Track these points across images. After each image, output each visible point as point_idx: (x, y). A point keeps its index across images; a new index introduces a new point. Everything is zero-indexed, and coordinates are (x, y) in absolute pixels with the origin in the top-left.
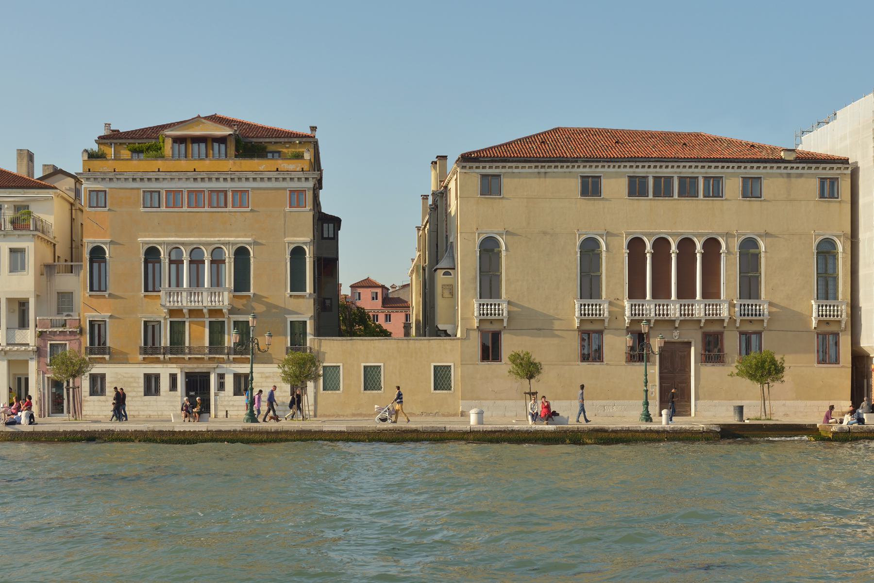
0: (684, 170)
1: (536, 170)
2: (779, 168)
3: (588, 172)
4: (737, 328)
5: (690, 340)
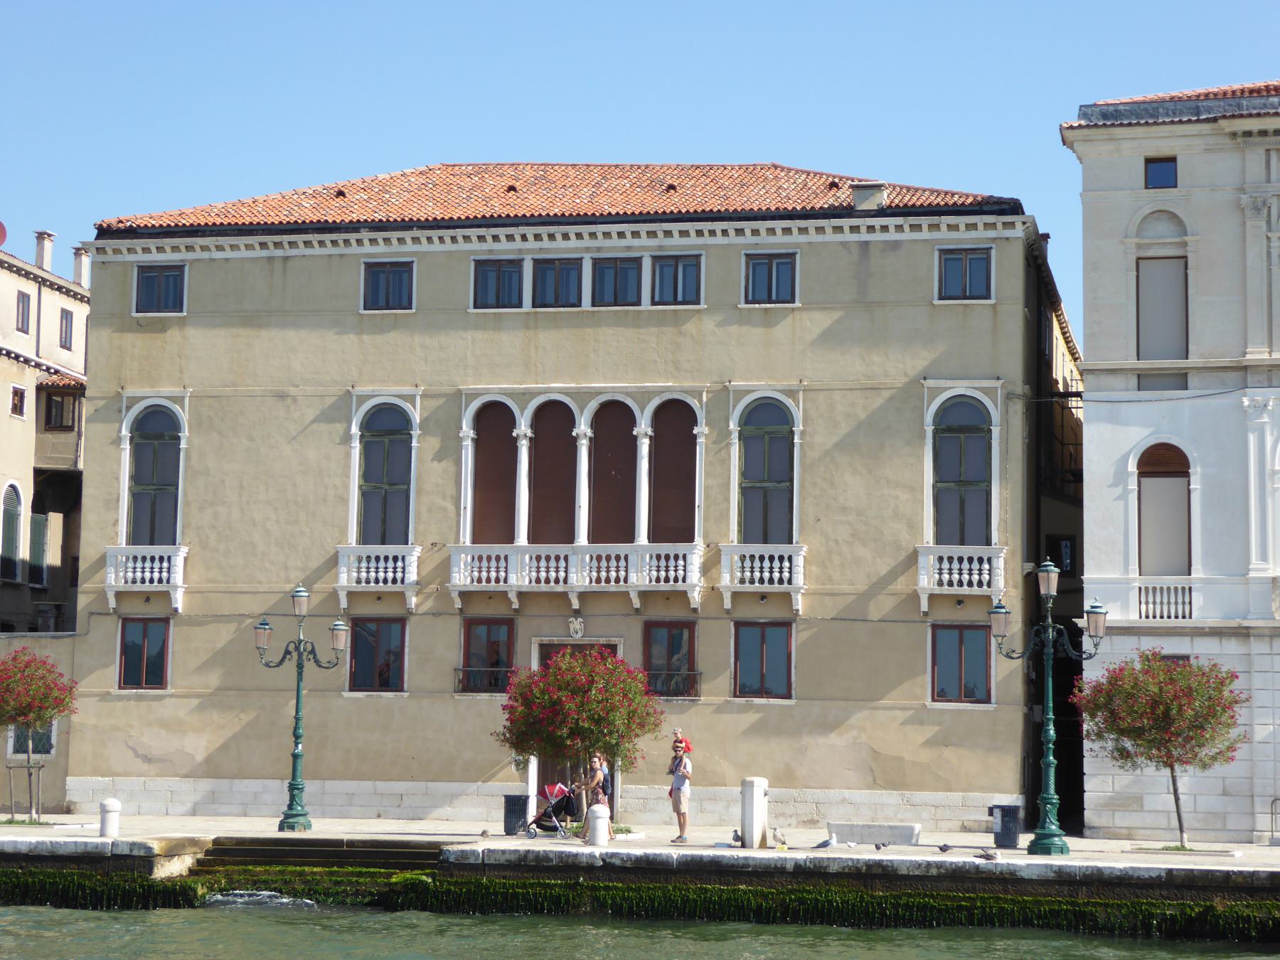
0: (608, 243)
1: (264, 253)
2: (839, 229)
3: (381, 255)
4: (728, 612)
5: (614, 640)
